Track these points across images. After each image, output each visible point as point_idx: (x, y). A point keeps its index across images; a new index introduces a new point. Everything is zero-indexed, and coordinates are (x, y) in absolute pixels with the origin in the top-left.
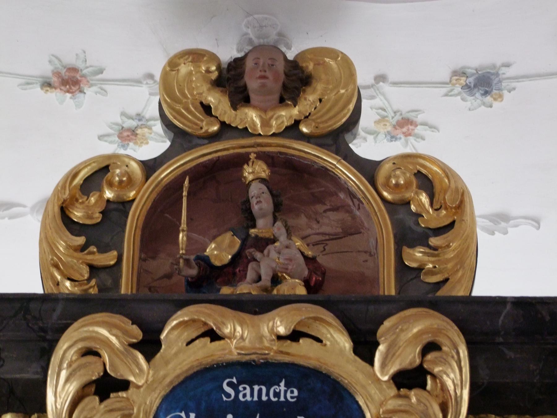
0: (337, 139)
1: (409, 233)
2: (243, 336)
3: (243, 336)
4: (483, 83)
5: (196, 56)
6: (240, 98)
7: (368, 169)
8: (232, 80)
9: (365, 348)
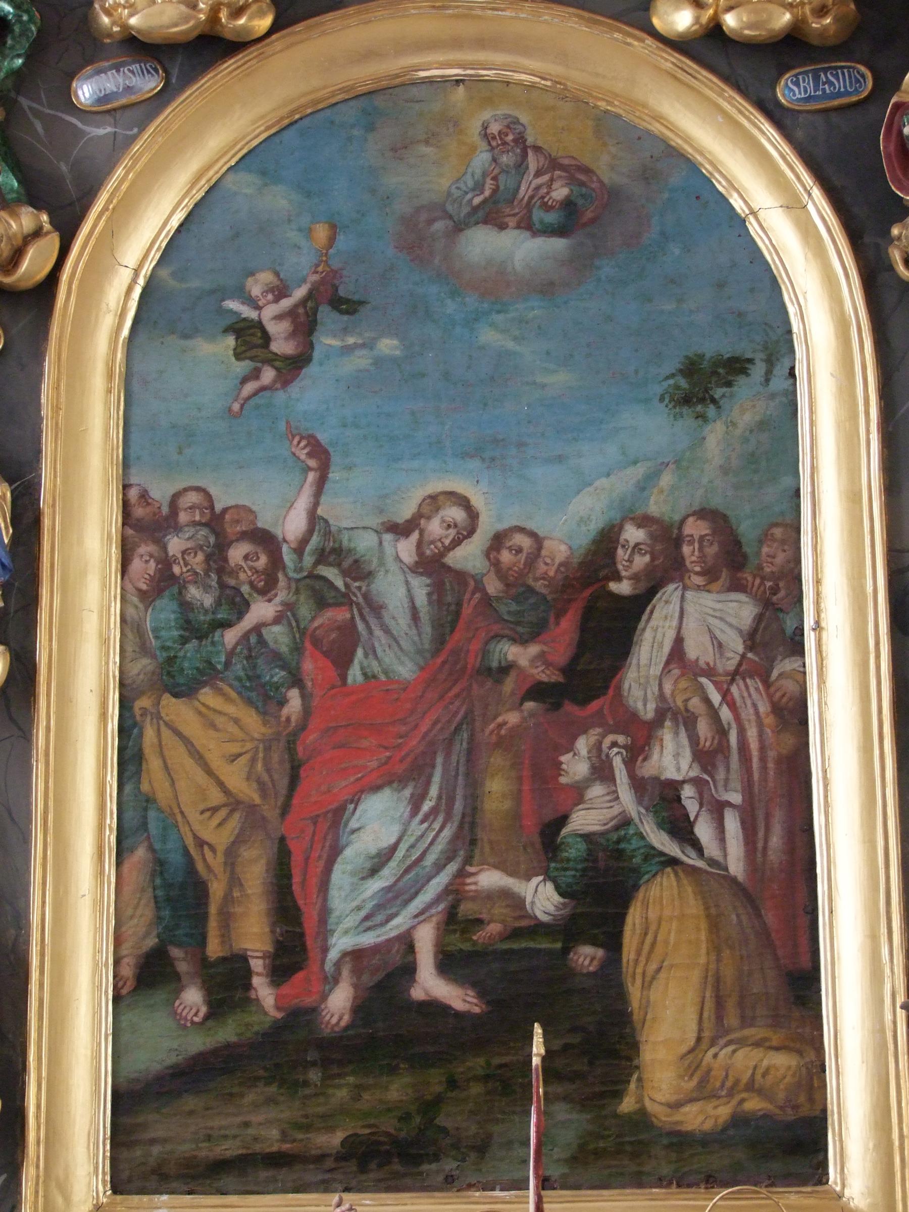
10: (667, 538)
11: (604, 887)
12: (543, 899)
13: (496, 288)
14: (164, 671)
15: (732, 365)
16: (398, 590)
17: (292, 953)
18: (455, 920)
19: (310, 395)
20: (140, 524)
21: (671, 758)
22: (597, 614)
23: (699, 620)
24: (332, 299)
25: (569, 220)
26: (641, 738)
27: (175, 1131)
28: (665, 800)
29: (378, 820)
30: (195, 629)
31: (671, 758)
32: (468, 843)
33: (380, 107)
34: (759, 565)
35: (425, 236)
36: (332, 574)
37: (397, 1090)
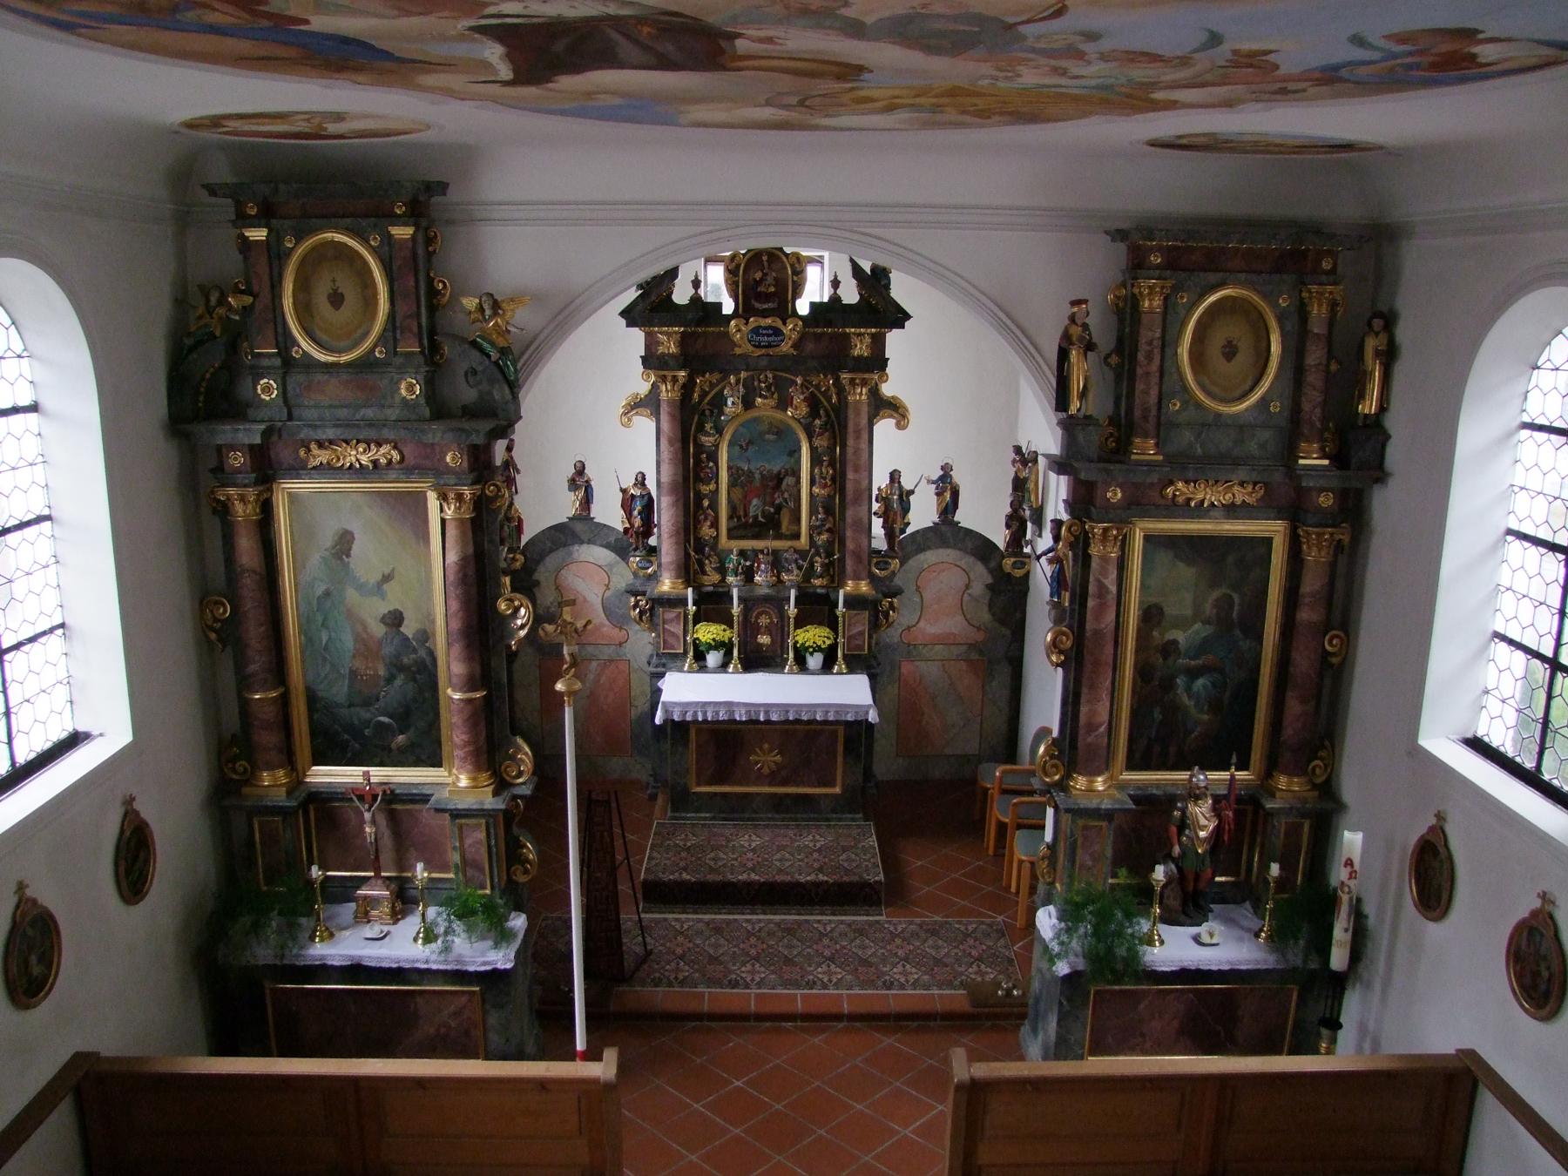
7: (787, 255)
11: (779, 509)
14: (732, 484)
15: (795, 452)
16: (757, 476)
17: (746, 515)
20: (729, 468)
22: (779, 479)
23: (789, 480)
24: (750, 442)
27: (735, 533)
29: (755, 502)
32: (765, 504)
33: (756, 420)
34: (796, 474)
35: (762, 434)
36: (750, 474)
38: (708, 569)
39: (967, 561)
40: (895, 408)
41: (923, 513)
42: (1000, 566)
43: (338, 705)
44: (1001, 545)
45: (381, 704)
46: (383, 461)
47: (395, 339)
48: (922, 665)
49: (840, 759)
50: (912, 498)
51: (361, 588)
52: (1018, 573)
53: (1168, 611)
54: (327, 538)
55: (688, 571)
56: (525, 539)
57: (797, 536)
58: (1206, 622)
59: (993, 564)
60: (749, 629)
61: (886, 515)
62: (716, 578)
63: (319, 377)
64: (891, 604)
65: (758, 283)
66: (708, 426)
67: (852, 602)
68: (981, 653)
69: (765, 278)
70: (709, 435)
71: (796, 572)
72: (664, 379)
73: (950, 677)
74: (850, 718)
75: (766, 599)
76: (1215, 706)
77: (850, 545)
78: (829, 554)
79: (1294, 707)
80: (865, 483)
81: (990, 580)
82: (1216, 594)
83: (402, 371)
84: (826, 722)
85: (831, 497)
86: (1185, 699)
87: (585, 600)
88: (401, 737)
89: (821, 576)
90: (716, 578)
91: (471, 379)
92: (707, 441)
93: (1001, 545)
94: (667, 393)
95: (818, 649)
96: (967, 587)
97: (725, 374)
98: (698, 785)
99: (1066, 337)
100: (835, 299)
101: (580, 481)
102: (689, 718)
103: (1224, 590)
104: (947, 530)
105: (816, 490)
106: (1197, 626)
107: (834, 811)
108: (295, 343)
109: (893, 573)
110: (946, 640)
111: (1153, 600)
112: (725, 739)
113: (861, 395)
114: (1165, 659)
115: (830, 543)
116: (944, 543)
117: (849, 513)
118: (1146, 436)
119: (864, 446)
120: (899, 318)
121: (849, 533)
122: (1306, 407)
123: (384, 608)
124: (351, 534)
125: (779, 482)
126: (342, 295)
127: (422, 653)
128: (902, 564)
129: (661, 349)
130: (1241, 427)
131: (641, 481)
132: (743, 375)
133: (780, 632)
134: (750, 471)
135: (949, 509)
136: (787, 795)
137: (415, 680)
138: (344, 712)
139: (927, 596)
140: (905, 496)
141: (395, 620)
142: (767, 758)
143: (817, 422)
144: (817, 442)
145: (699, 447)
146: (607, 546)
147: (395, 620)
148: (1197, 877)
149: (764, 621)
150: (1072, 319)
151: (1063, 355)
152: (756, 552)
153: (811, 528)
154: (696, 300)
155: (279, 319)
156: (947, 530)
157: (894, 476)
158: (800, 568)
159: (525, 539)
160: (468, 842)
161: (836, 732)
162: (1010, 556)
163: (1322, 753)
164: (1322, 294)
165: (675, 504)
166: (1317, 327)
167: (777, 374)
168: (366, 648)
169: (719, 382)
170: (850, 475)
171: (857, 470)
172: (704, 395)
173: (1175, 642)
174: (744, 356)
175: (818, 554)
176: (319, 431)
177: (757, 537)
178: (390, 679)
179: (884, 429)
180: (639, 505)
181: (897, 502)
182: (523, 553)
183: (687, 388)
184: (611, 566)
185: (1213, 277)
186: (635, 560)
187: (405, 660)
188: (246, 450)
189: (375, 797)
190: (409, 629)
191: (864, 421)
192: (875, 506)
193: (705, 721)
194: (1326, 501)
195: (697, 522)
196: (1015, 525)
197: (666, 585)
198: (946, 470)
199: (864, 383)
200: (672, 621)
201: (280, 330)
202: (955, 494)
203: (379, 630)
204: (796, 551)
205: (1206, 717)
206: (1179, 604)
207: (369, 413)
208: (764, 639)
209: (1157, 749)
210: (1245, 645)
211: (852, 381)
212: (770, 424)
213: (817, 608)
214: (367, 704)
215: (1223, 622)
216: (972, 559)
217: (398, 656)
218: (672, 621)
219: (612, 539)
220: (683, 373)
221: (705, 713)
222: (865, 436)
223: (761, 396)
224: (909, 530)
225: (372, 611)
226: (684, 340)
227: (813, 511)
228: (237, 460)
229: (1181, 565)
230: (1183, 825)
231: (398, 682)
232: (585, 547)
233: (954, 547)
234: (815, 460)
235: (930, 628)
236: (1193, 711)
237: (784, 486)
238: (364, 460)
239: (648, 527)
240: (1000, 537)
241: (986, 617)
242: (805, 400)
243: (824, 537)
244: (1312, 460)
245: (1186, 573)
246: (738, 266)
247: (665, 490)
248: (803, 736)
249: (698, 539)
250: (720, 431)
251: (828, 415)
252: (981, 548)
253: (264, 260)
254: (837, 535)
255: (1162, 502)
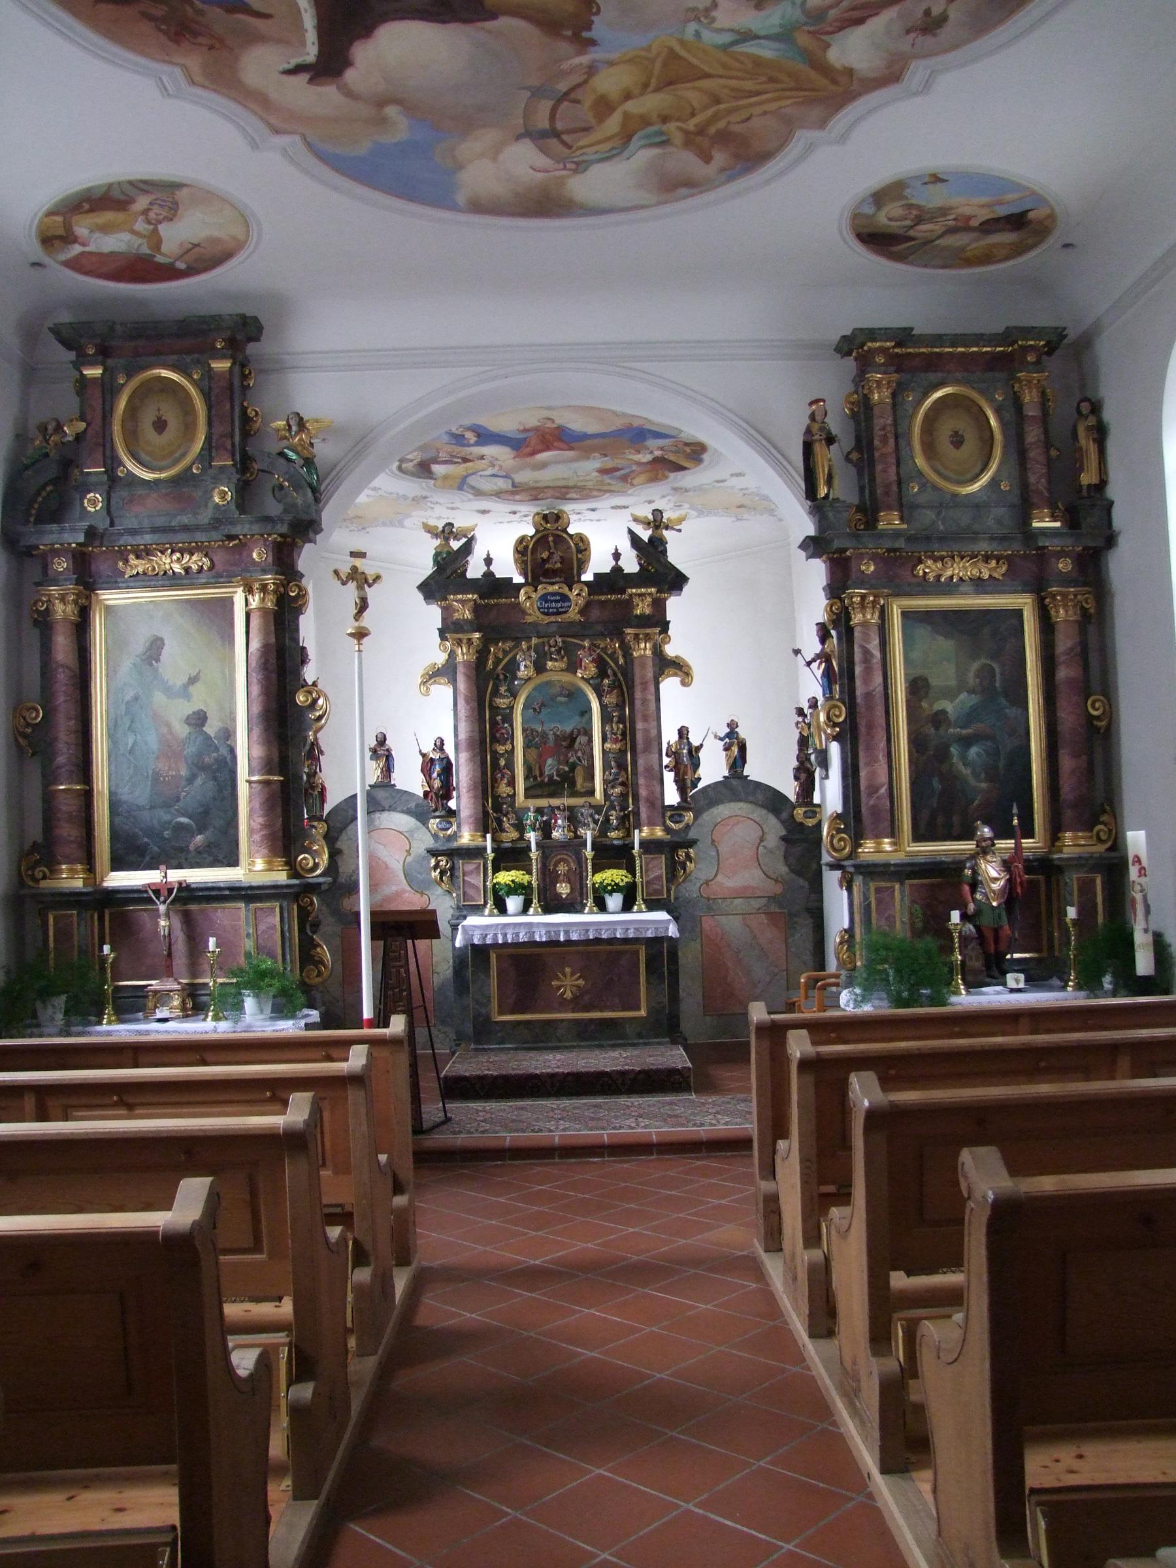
0: (565, 531)
1: (579, 551)
2: (551, 589)
3: (551, 589)
4: (593, 510)
5: (538, 514)
6: (547, 522)
7: (571, 536)
8: (545, 518)
9: (571, 590)
10: (579, 731)
11: (573, 767)
12: (567, 769)
13: (561, 703)
14: (527, 746)
15: (586, 712)
16: (551, 737)
17: (541, 774)
18: (558, 771)
19: (541, 716)
20: (524, 730)
21: (580, 754)
22: (571, 739)
23: (582, 739)
24: (543, 705)
25: (568, 696)
26: (576, 752)
27: (531, 793)
28: (579, 759)
29: (549, 761)
30: (530, 741)
31: (580, 754)
32: (559, 763)
33: (549, 684)
34: (588, 733)
35: (553, 699)
36: (544, 735)
37: (552, 788)
38: (506, 825)
39: (760, 814)
40: (679, 667)
41: (712, 768)
42: (792, 816)
43: (139, 808)
44: (792, 797)
45: (181, 804)
46: (195, 567)
47: (210, 455)
48: (723, 919)
49: (643, 979)
50: (701, 754)
51: (168, 691)
52: (810, 823)
53: (933, 682)
54: (139, 645)
55: (484, 824)
56: (328, 808)
57: (592, 793)
58: (971, 691)
59: (784, 815)
60: (549, 877)
61: (676, 768)
62: (515, 835)
63: (140, 491)
64: (688, 855)
65: (544, 561)
66: (502, 689)
67: (646, 845)
68: (781, 906)
69: (552, 554)
70: (504, 697)
71: (592, 825)
72: (459, 643)
73: (751, 932)
74: (649, 934)
75: (564, 846)
76: (992, 775)
77: (643, 792)
78: (624, 808)
79: (1067, 763)
80: (654, 732)
81: (784, 833)
82: (975, 666)
83: (216, 481)
84: (626, 941)
85: (622, 752)
86: (961, 767)
87: (387, 867)
88: (199, 838)
89: (617, 829)
90: (515, 835)
91: (277, 494)
92: (502, 702)
93: (792, 797)
94: (463, 655)
95: (616, 888)
96: (762, 840)
97: (517, 640)
98: (501, 1013)
99: (808, 431)
100: (617, 570)
101: (382, 752)
102: (489, 941)
103: (984, 661)
104: (737, 783)
105: (608, 745)
106: (963, 696)
107: (639, 1035)
108: (121, 464)
109: (688, 827)
110: (744, 893)
111: (918, 672)
112: (527, 964)
113: (644, 650)
114: (937, 728)
115: (624, 796)
116: (736, 798)
117: (641, 762)
118: (889, 508)
119: (652, 698)
120: (676, 581)
121: (641, 781)
122: (1032, 479)
123: (188, 708)
124: (162, 640)
125: (573, 742)
126: (165, 422)
127: (224, 751)
128: (696, 818)
129: (456, 616)
130: (977, 506)
131: (440, 745)
132: (534, 641)
133: (577, 879)
134: (544, 732)
135: (738, 762)
136: (591, 1020)
137: (215, 779)
138: (146, 815)
139: (723, 849)
140: (694, 752)
141: (199, 719)
142: (568, 983)
143: (606, 681)
144: (606, 700)
145: (494, 709)
146: (408, 812)
147: (199, 719)
148: (996, 931)
149: (562, 869)
150: (813, 417)
151: (808, 448)
152: (552, 809)
153: (606, 782)
154: (489, 575)
155: (108, 446)
156: (737, 783)
157: (683, 733)
158: (596, 822)
159: (328, 808)
160: (262, 927)
161: (637, 952)
162: (800, 806)
163: (1104, 818)
164: (1030, 382)
165: (472, 759)
166: (1031, 411)
167: (565, 640)
168: (169, 749)
169: (511, 650)
170: (640, 726)
171: (646, 719)
172: (497, 661)
173: (943, 712)
174: (535, 624)
175: (612, 807)
176: (138, 538)
177: (552, 795)
178: (191, 780)
179: (670, 686)
180: (438, 769)
181: (686, 759)
182: (326, 821)
183: (482, 654)
184: (411, 831)
185: (933, 377)
186: (434, 823)
187: (207, 759)
188: (70, 556)
189: (170, 891)
190: (211, 729)
191: (650, 675)
192: (666, 760)
193: (506, 945)
194: (1064, 566)
195: (494, 781)
196: (803, 776)
197: (466, 838)
198: (732, 726)
199: (647, 638)
200: (471, 872)
201: (108, 452)
202: (743, 748)
203: (182, 730)
204: (591, 806)
205: (984, 785)
206: (943, 675)
207: (185, 519)
208: (563, 889)
209: (940, 820)
210: (1012, 712)
211: (636, 636)
212: (562, 687)
213: (612, 854)
214: (166, 805)
215: (987, 689)
216: (764, 812)
217: (200, 755)
218: (471, 872)
219: (412, 805)
220: (477, 635)
221: (505, 935)
222: (652, 688)
223: (551, 659)
224: (701, 785)
225: (176, 713)
226: (477, 609)
227: (606, 767)
228: (61, 565)
229: (941, 639)
230: (974, 885)
231: (199, 781)
232: (386, 814)
233: (746, 801)
234: (606, 719)
235: (728, 882)
236: (972, 781)
237: (576, 745)
238: (177, 568)
239: (446, 791)
240: (789, 789)
241: (784, 869)
242: (593, 661)
243: (618, 790)
244: (1043, 523)
245: (945, 645)
246: (526, 547)
247: (463, 745)
248: (605, 958)
249: (496, 798)
250: (514, 695)
251: (615, 674)
252: (773, 800)
253: (98, 394)
254: (630, 789)
255: (914, 580)
